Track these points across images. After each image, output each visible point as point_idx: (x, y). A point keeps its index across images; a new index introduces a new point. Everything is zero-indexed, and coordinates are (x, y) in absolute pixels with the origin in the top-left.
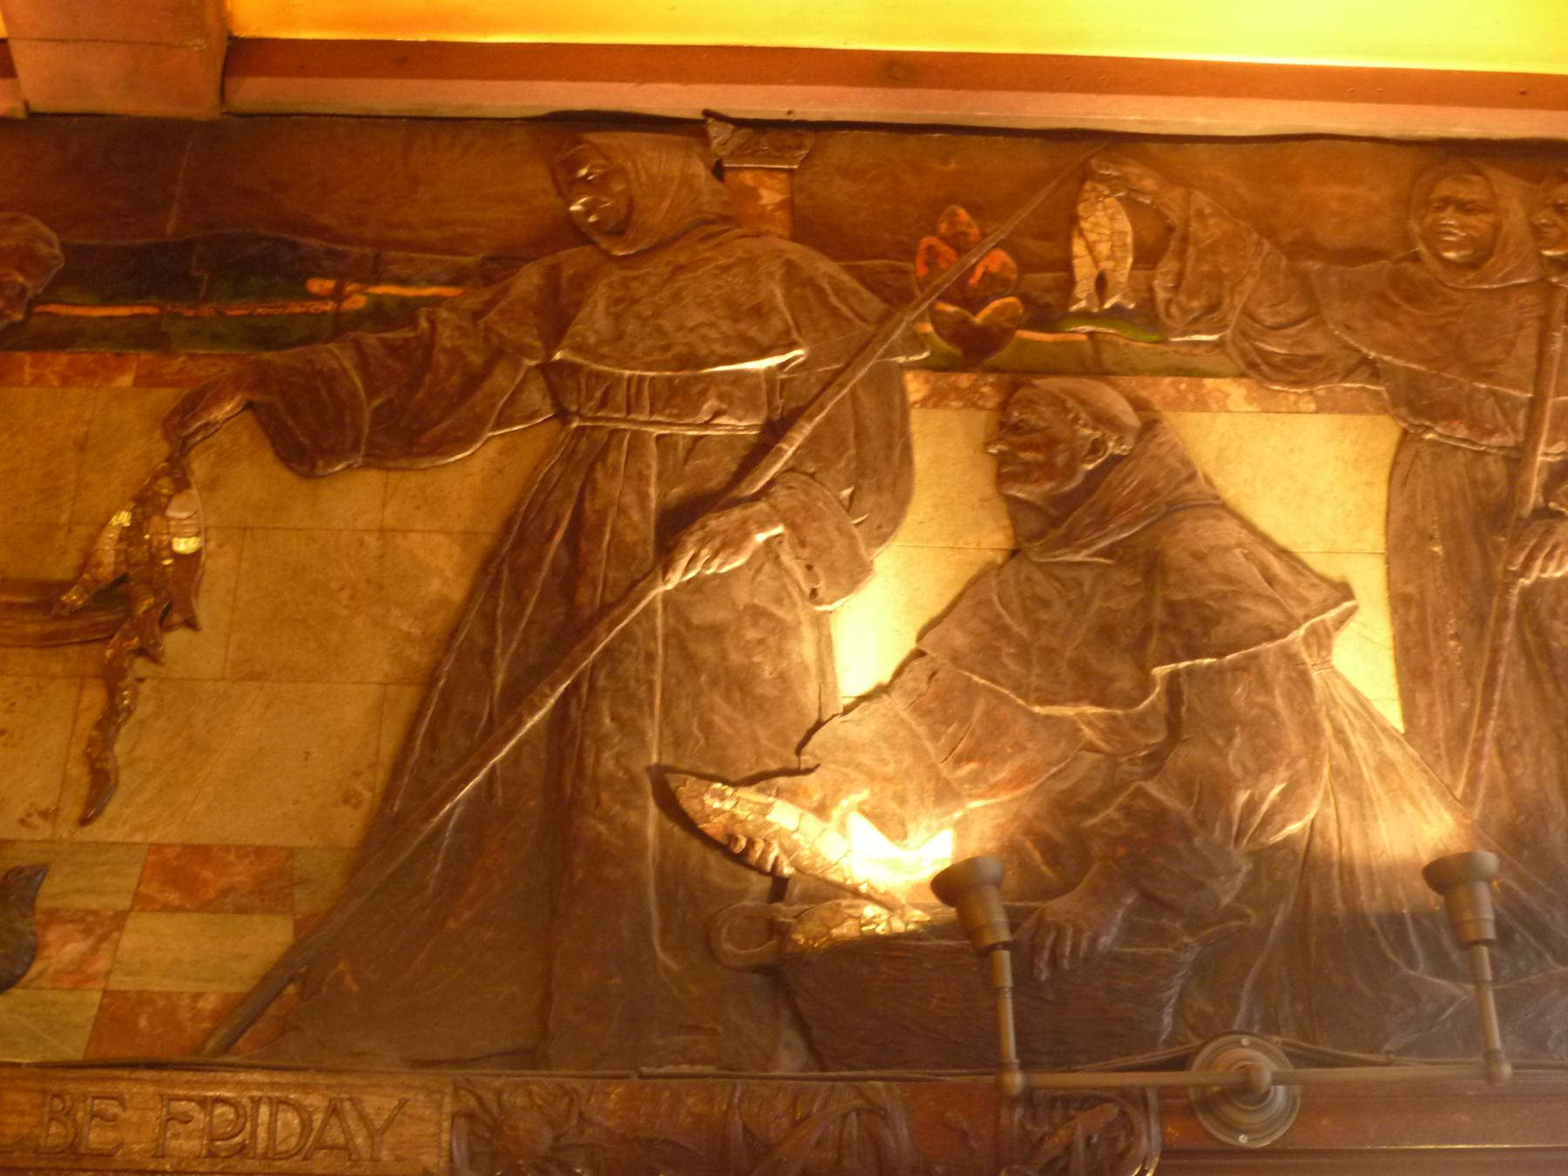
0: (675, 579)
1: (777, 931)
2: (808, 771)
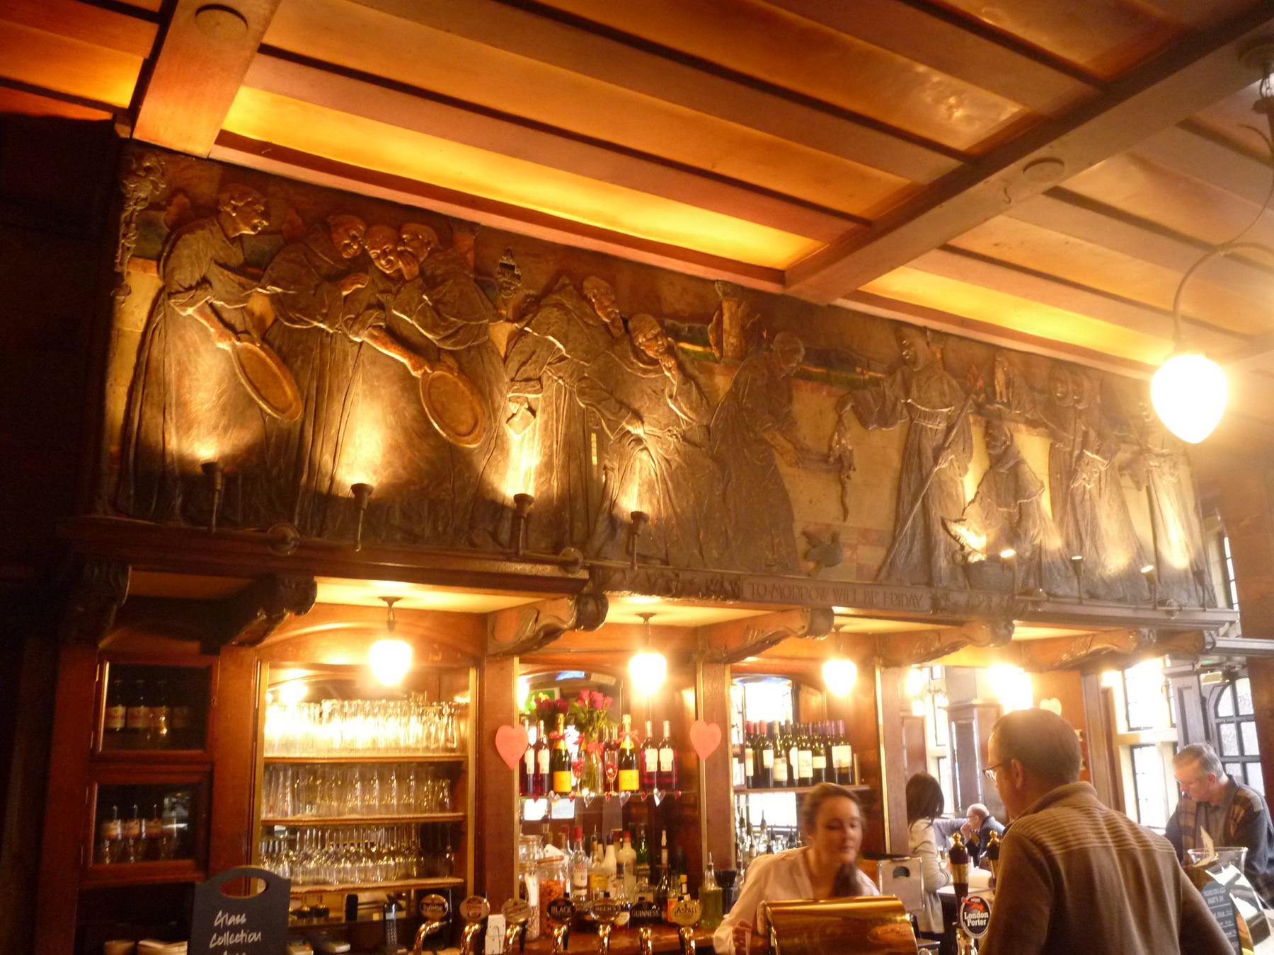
0: (938, 468)
1: (965, 558)
2: (965, 520)
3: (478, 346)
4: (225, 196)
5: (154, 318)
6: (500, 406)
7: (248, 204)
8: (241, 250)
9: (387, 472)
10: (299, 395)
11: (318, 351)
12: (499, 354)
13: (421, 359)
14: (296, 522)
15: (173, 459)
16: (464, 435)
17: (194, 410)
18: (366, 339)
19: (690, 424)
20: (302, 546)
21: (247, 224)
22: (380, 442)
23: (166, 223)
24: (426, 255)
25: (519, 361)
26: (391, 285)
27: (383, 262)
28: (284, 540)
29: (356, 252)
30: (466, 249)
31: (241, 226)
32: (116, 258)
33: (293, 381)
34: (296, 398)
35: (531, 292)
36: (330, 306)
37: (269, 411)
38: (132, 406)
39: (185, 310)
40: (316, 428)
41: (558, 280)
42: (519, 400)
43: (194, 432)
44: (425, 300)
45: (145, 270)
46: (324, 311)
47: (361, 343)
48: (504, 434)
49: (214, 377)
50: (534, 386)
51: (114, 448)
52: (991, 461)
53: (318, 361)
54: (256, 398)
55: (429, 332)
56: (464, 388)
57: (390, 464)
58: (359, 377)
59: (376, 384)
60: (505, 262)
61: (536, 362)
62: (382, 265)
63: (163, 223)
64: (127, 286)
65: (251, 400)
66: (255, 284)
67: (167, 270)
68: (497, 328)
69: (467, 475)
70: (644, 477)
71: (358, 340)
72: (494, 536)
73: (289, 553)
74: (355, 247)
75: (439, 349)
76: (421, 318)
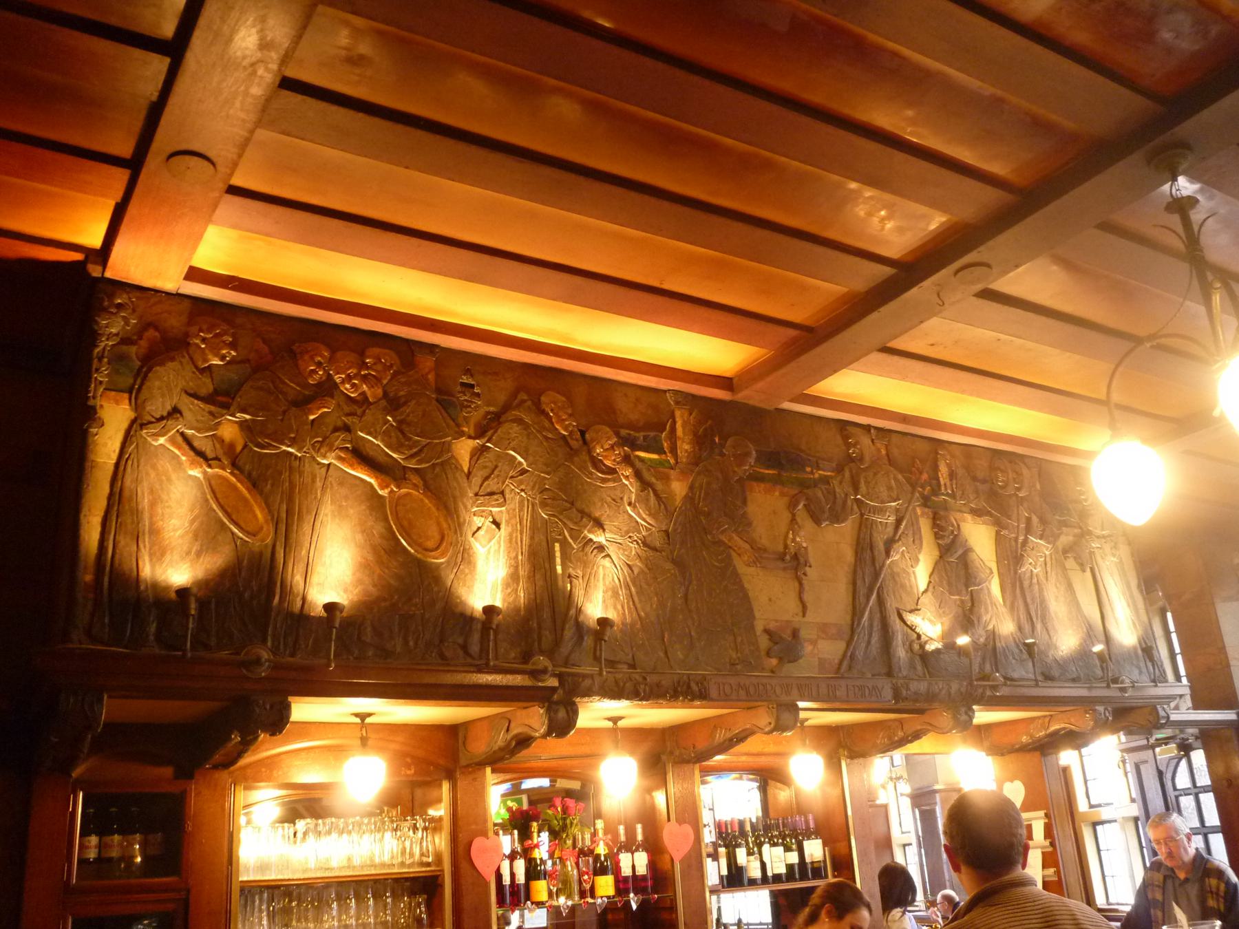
1: (922, 647)
2: (919, 610)
3: (442, 464)
4: (194, 329)
5: (126, 450)
6: (465, 520)
7: (216, 336)
8: (210, 380)
9: (357, 590)
10: (270, 518)
11: (287, 474)
12: (463, 471)
13: (387, 479)
14: (269, 644)
15: (147, 587)
16: (432, 551)
17: (167, 537)
18: (333, 461)
19: (650, 529)
20: (276, 667)
21: (216, 355)
22: (350, 561)
23: (138, 357)
24: (389, 377)
25: (482, 477)
26: (356, 407)
27: (348, 386)
28: (258, 662)
29: (321, 378)
30: (427, 370)
31: (210, 357)
32: (89, 392)
33: (263, 504)
34: (266, 521)
35: (492, 409)
36: (297, 431)
37: (241, 535)
38: (106, 536)
39: (157, 440)
40: (287, 549)
41: (516, 398)
42: (484, 514)
43: (168, 557)
44: (389, 421)
45: (117, 402)
46: (292, 435)
47: (329, 465)
48: (471, 548)
49: (186, 504)
50: (497, 500)
51: (88, 578)
52: (940, 551)
53: (287, 484)
54: (228, 523)
55: (394, 453)
56: (430, 505)
57: (360, 582)
58: (328, 498)
59: (344, 504)
60: (465, 381)
61: (498, 476)
62: (346, 389)
63: (134, 357)
64: (100, 418)
65: (223, 524)
66: (225, 412)
67: (139, 401)
68: (459, 446)
69: (436, 589)
70: (607, 583)
71: (325, 462)
72: (465, 647)
73: (263, 674)
74: (321, 373)
75: (404, 467)
76: (386, 438)
